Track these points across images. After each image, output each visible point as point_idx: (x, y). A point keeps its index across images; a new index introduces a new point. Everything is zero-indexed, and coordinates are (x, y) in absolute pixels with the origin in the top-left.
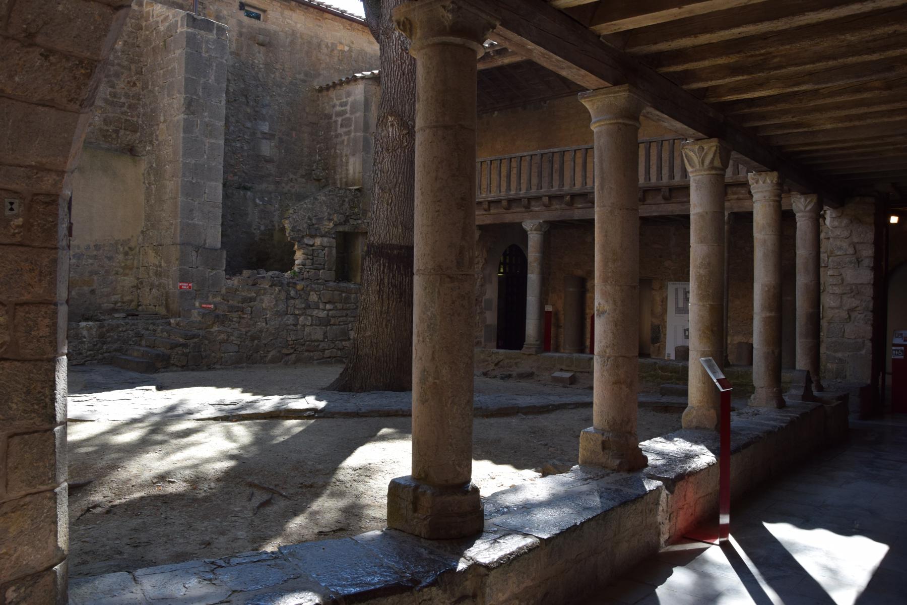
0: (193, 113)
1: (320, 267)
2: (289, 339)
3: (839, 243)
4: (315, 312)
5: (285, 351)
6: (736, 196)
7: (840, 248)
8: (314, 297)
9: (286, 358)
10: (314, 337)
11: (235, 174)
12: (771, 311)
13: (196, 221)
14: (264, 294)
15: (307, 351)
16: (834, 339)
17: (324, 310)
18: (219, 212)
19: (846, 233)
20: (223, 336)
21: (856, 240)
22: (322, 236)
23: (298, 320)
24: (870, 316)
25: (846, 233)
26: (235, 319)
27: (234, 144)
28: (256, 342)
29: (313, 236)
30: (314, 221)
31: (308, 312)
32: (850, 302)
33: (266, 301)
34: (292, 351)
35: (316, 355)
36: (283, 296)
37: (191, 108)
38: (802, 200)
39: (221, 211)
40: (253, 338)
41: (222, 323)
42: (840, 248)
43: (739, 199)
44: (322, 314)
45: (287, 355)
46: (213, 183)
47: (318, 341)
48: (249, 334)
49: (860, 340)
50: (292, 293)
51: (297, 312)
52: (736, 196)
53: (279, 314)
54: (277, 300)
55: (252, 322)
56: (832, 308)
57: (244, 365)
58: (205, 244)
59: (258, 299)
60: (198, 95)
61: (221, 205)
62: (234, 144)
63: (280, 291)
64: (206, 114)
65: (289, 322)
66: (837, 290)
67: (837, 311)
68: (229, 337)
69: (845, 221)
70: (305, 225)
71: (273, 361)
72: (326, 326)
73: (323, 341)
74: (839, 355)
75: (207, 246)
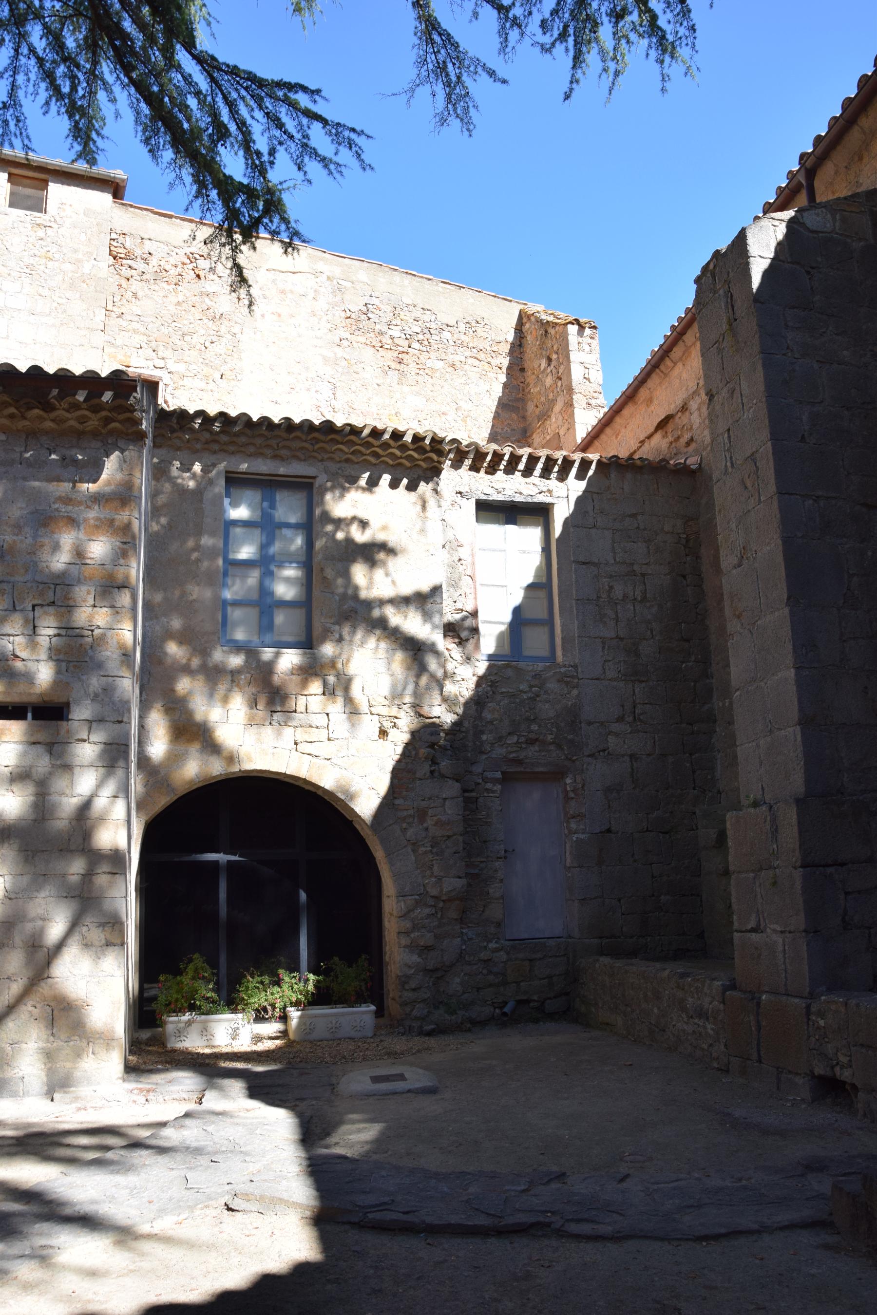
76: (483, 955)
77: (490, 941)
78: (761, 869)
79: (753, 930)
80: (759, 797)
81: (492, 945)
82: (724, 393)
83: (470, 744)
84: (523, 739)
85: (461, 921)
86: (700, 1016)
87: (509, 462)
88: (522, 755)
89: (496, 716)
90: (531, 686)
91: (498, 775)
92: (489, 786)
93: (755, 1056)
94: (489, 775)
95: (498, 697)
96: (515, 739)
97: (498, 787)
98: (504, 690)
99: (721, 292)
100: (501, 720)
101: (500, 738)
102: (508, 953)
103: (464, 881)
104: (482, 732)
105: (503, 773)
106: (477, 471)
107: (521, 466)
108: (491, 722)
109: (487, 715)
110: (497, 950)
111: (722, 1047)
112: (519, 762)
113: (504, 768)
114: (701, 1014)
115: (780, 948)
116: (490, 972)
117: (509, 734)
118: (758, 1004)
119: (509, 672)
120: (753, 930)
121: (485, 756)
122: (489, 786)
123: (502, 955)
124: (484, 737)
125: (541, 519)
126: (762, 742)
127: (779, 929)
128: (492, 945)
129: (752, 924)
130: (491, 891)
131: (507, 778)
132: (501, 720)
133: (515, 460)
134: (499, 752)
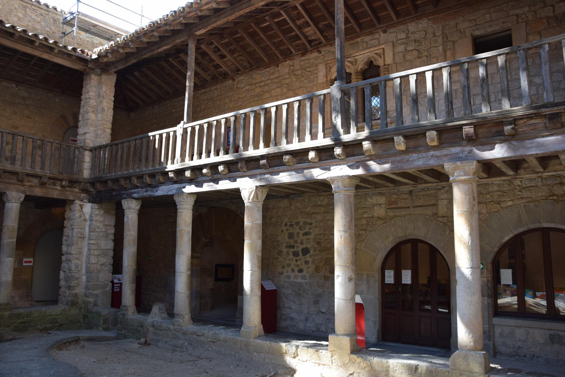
3: (98, 224)
6: (29, 184)
7: (98, 228)
16: (93, 283)
19: (102, 219)
21: (106, 224)
24: (111, 268)
25: (102, 219)
32: (103, 260)
38: (134, 202)
42: (98, 228)
43: (31, 186)
49: (106, 282)
52: (29, 184)
56: (93, 264)
66: (96, 253)
67: (95, 265)
69: (102, 212)
74: (96, 292)
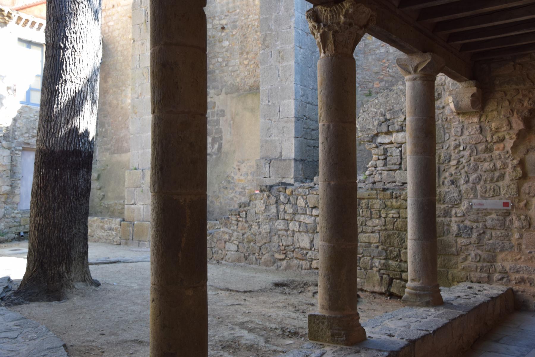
0: (267, 47)
1: (395, 167)
2: (281, 244)
4: (302, 218)
5: (277, 256)
8: (301, 202)
9: (279, 263)
10: (302, 245)
11: (381, 80)
12: (325, 241)
13: (273, 138)
14: (256, 199)
15: (296, 258)
17: (312, 215)
18: (292, 126)
20: (227, 237)
22: (398, 131)
23: (288, 226)
26: (233, 222)
27: (378, 51)
28: (252, 244)
29: (389, 133)
30: (388, 117)
31: (297, 217)
33: (258, 206)
34: (283, 256)
35: (304, 262)
36: (273, 200)
37: (266, 43)
39: (293, 124)
40: (249, 242)
41: (226, 225)
44: (309, 220)
45: (280, 260)
46: (286, 101)
47: (306, 249)
48: (245, 236)
50: (282, 198)
51: (287, 218)
53: (270, 219)
54: (267, 206)
55: (246, 225)
57: (242, 264)
58: (281, 156)
59: (252, 203)
60: (271, 30)
61: (293, 119)
62: (378, 51)
63: (268, 196)
64: (278, 43)
65: (280, 227)
68: (231, 237)
70: (376, 123)
71: (266, 264)
72: (313, 233)
73: (311, 249)
75: (282, 158)
76: (13, 215)
77: (15, 210)
78: (137, 187)
79: (132, 204)
80: (137, 167)
81: (16, 212)
82: (140, 42)
83: (11, 135)
84: (30, 135)
85: (5, 203)
86: (110, 230)
87: (32, 24)
88: (30, 141)
89: (21, 125)
90: (35, 116)
91: (21, 148)
92: (17, 152)
93: (131, 238)
94: (18, 148)
95: (22, 118)
96: (27, 135)
97: (20, 153)
98: (24, 116)
99: (143, 9)
100: (23, 127)
101: (22, 134)
102: (22, 214)
103: (10, 187)
104: (15, 131)
105: (23, 147)
106: (18, 24)
107: (36, 26)
108: (19, 128)
109: (18, 125)
110: (17, 213)
111: (118, 238)
112: (28, 144)
113: (23, 146)
114: (110, 229)
115: (142, 209)
116: (15, 221)
117: (26, 133)
118: (134, 224)
119: (27, 109)
120: (132, 204)
121: (16, 141)
122: (17, 152)
123: (20, 215)
124: (16, 133)
125: (40, 49)
126: (140, 151)
127: (142, 203)
128: (16, 212)
129: (133, 202)
130: (16, 191)
131: (24, 149)
132: (23, 127)
133: (33, 23)
134: (21, 139)
